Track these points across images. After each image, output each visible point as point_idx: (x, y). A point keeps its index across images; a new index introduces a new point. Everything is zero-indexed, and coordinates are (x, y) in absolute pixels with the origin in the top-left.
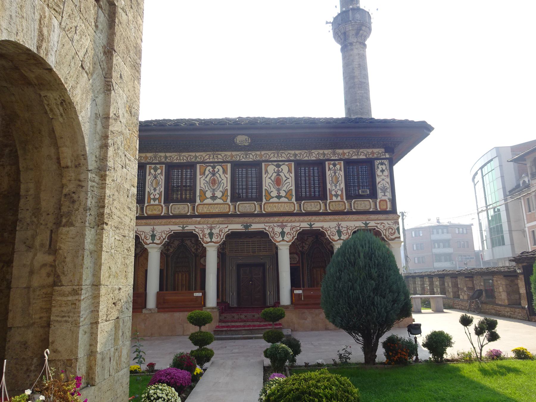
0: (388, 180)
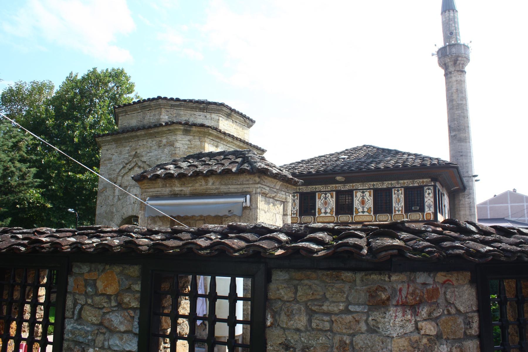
0: (432, 200)
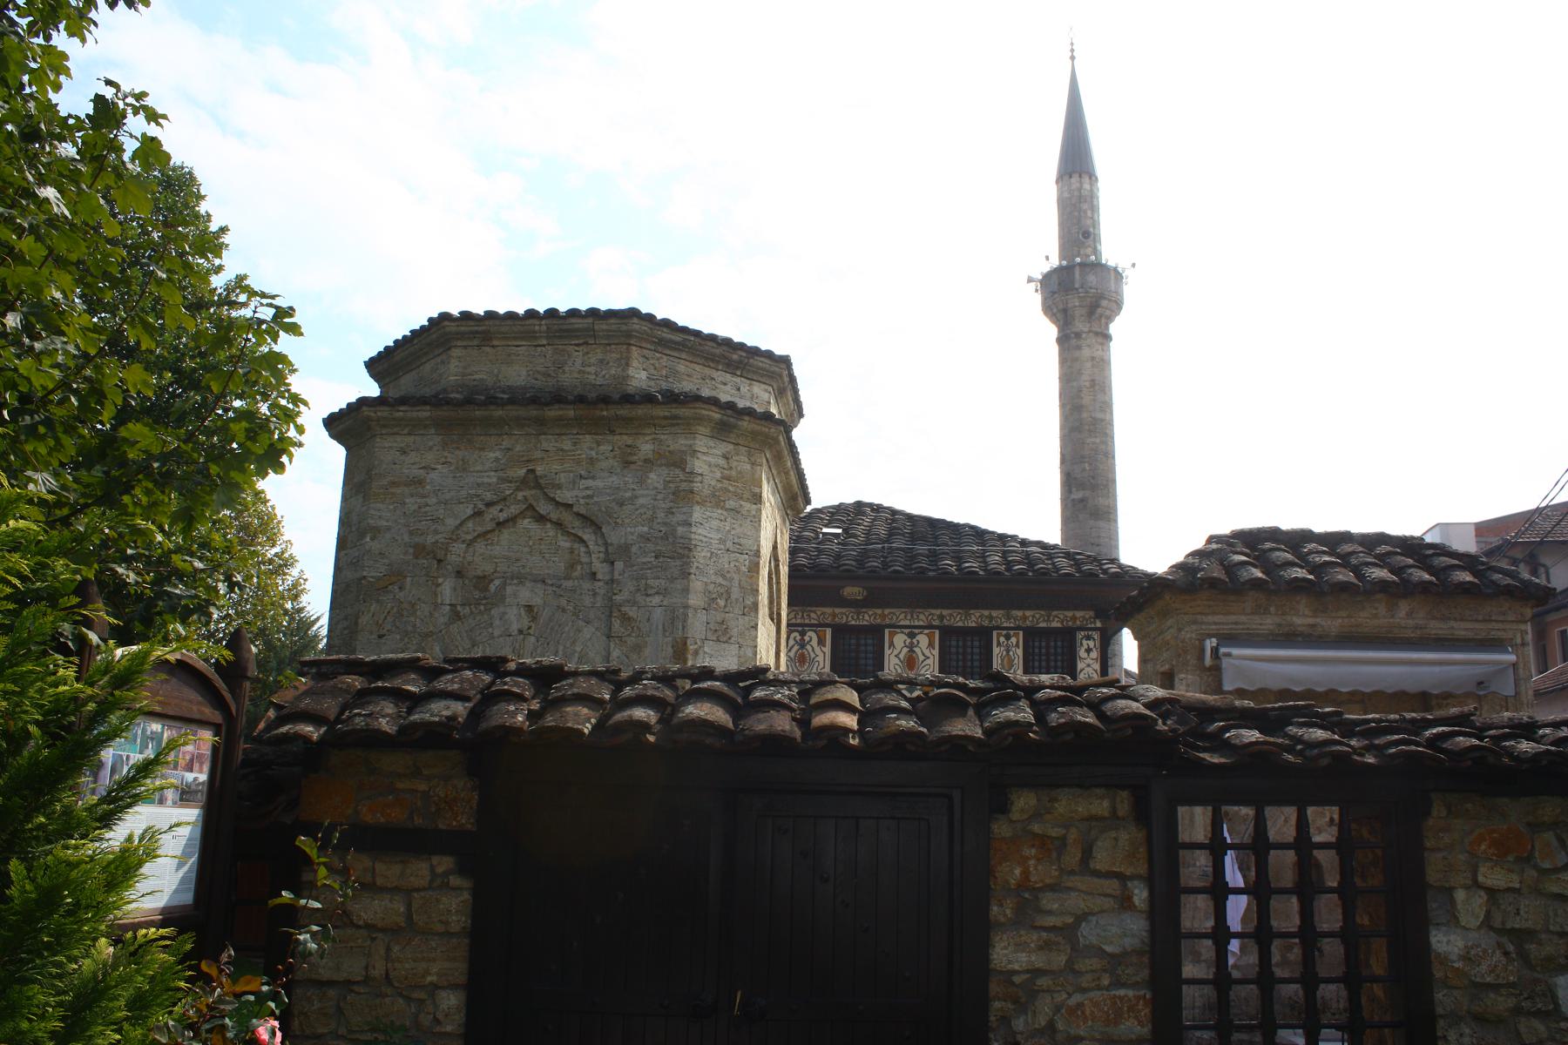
0: (1097, 666)
